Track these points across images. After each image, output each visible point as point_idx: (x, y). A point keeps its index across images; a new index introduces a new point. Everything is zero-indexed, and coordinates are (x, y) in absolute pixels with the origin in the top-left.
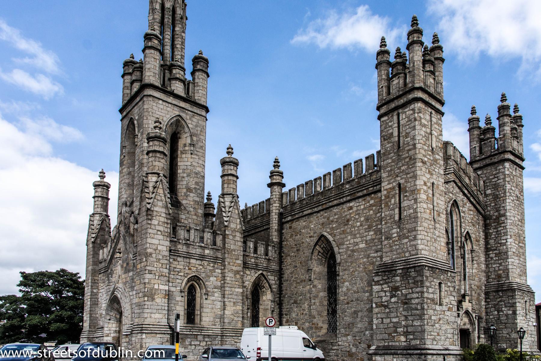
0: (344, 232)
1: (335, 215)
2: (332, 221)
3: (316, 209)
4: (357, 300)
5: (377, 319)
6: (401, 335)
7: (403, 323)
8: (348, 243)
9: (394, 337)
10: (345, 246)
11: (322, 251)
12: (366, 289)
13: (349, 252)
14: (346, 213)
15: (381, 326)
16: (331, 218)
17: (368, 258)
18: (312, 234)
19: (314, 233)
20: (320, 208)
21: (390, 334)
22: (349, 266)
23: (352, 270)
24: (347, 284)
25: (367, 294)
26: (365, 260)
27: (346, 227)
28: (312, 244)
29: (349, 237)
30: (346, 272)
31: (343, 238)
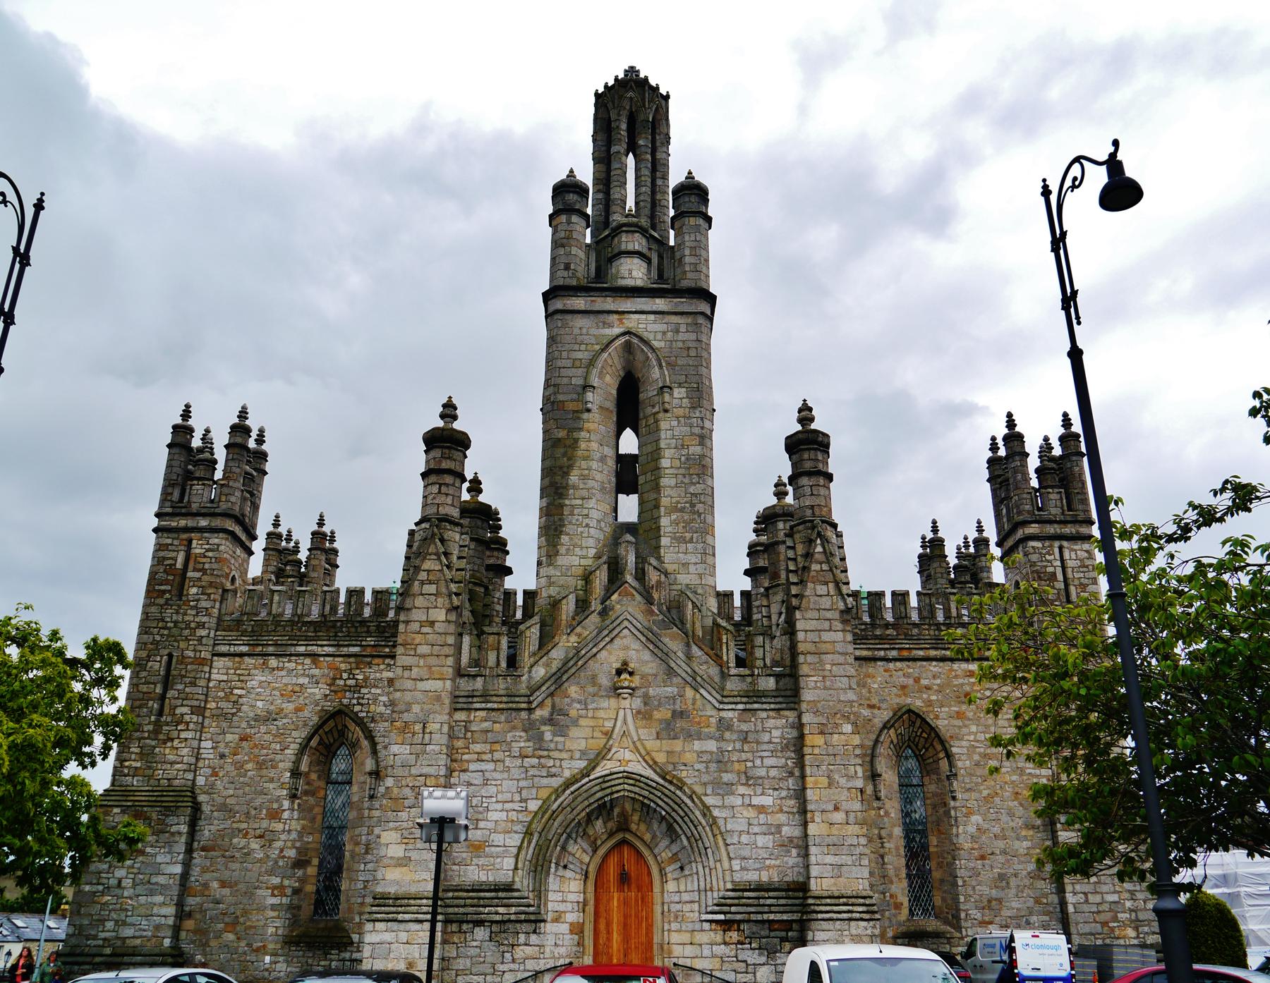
0: (959, 715)
1: (934, 677)
2: (928, 688)
3: (882, 653)
4: (1004, 852)
5: (1075, 894)
6: (1125, 926)
7: (1128, 904)
8: (972, 738)
9: (1112, 929)
10: (964, 743)
11: (895, 741)
12: (1024, 833)
13: (976, 757)
14: (961, 681)
15: (1086, 908)
16: (924, 682)
17: (1021, 775)
18: (874, 701)
19: (881, 701)
20: (894, 653)
21: (1104, 924)
22: (977, 784)
23: (985, 793)
24: (976, 819)
25: (1026, 844)
26: (1014, 778)
27: (964, 707)
28: (878, 723)
29: (974, 728)
30: (974, 795)
31: (960, 727)
